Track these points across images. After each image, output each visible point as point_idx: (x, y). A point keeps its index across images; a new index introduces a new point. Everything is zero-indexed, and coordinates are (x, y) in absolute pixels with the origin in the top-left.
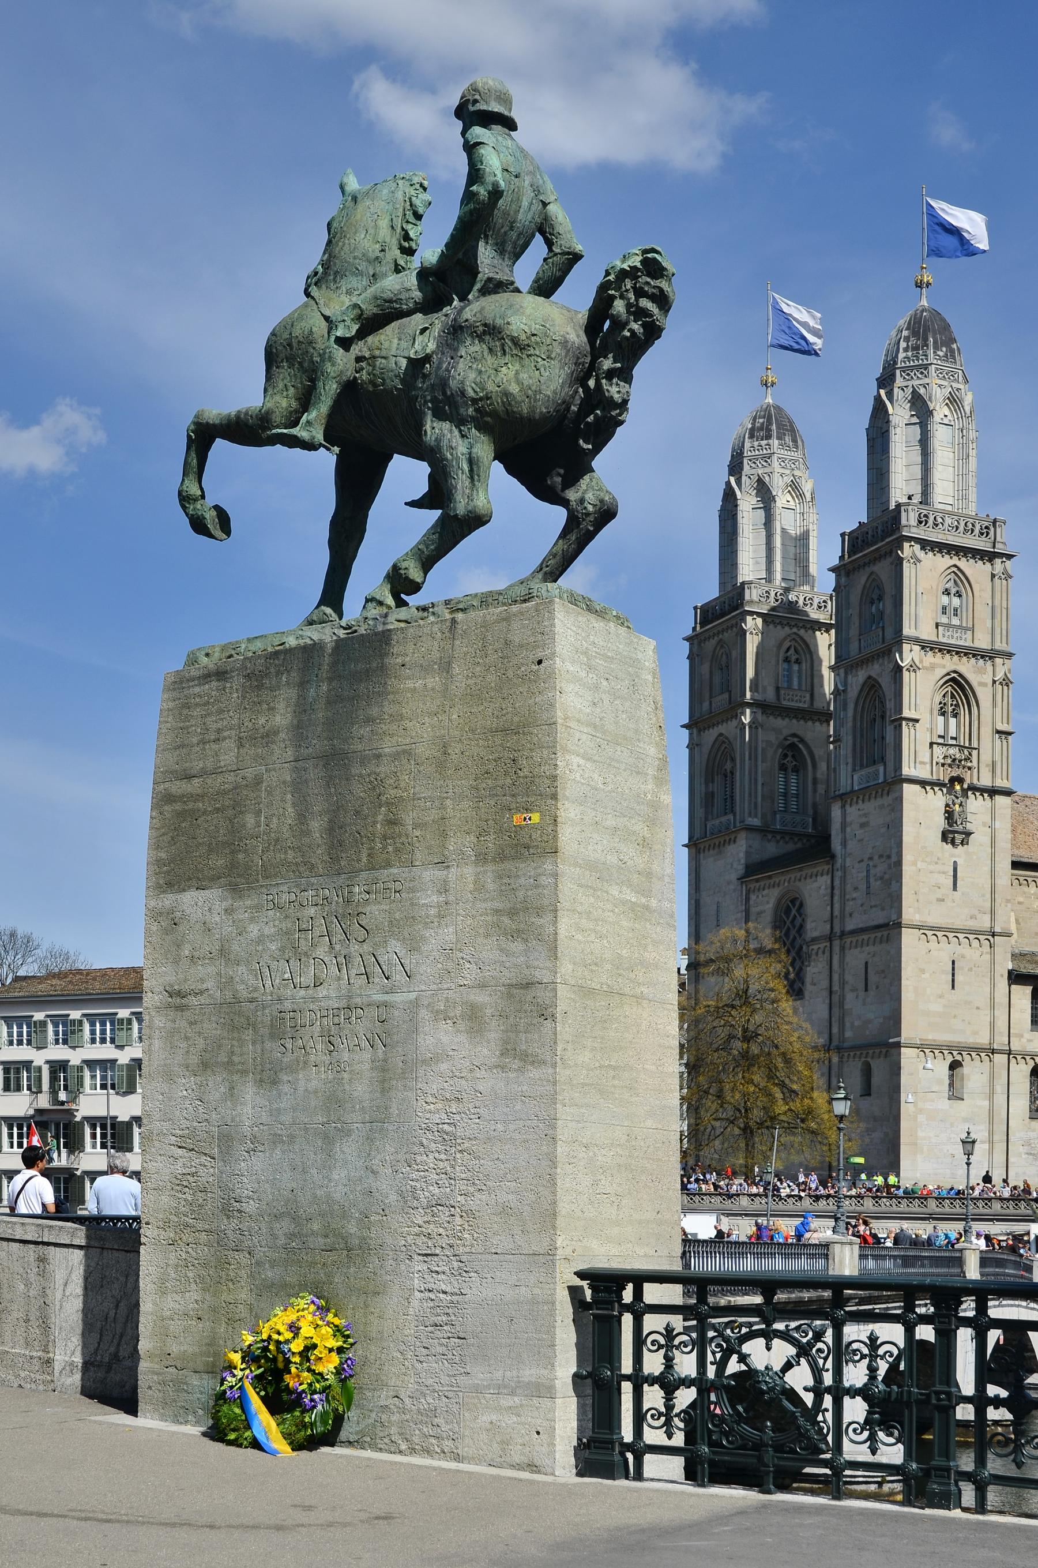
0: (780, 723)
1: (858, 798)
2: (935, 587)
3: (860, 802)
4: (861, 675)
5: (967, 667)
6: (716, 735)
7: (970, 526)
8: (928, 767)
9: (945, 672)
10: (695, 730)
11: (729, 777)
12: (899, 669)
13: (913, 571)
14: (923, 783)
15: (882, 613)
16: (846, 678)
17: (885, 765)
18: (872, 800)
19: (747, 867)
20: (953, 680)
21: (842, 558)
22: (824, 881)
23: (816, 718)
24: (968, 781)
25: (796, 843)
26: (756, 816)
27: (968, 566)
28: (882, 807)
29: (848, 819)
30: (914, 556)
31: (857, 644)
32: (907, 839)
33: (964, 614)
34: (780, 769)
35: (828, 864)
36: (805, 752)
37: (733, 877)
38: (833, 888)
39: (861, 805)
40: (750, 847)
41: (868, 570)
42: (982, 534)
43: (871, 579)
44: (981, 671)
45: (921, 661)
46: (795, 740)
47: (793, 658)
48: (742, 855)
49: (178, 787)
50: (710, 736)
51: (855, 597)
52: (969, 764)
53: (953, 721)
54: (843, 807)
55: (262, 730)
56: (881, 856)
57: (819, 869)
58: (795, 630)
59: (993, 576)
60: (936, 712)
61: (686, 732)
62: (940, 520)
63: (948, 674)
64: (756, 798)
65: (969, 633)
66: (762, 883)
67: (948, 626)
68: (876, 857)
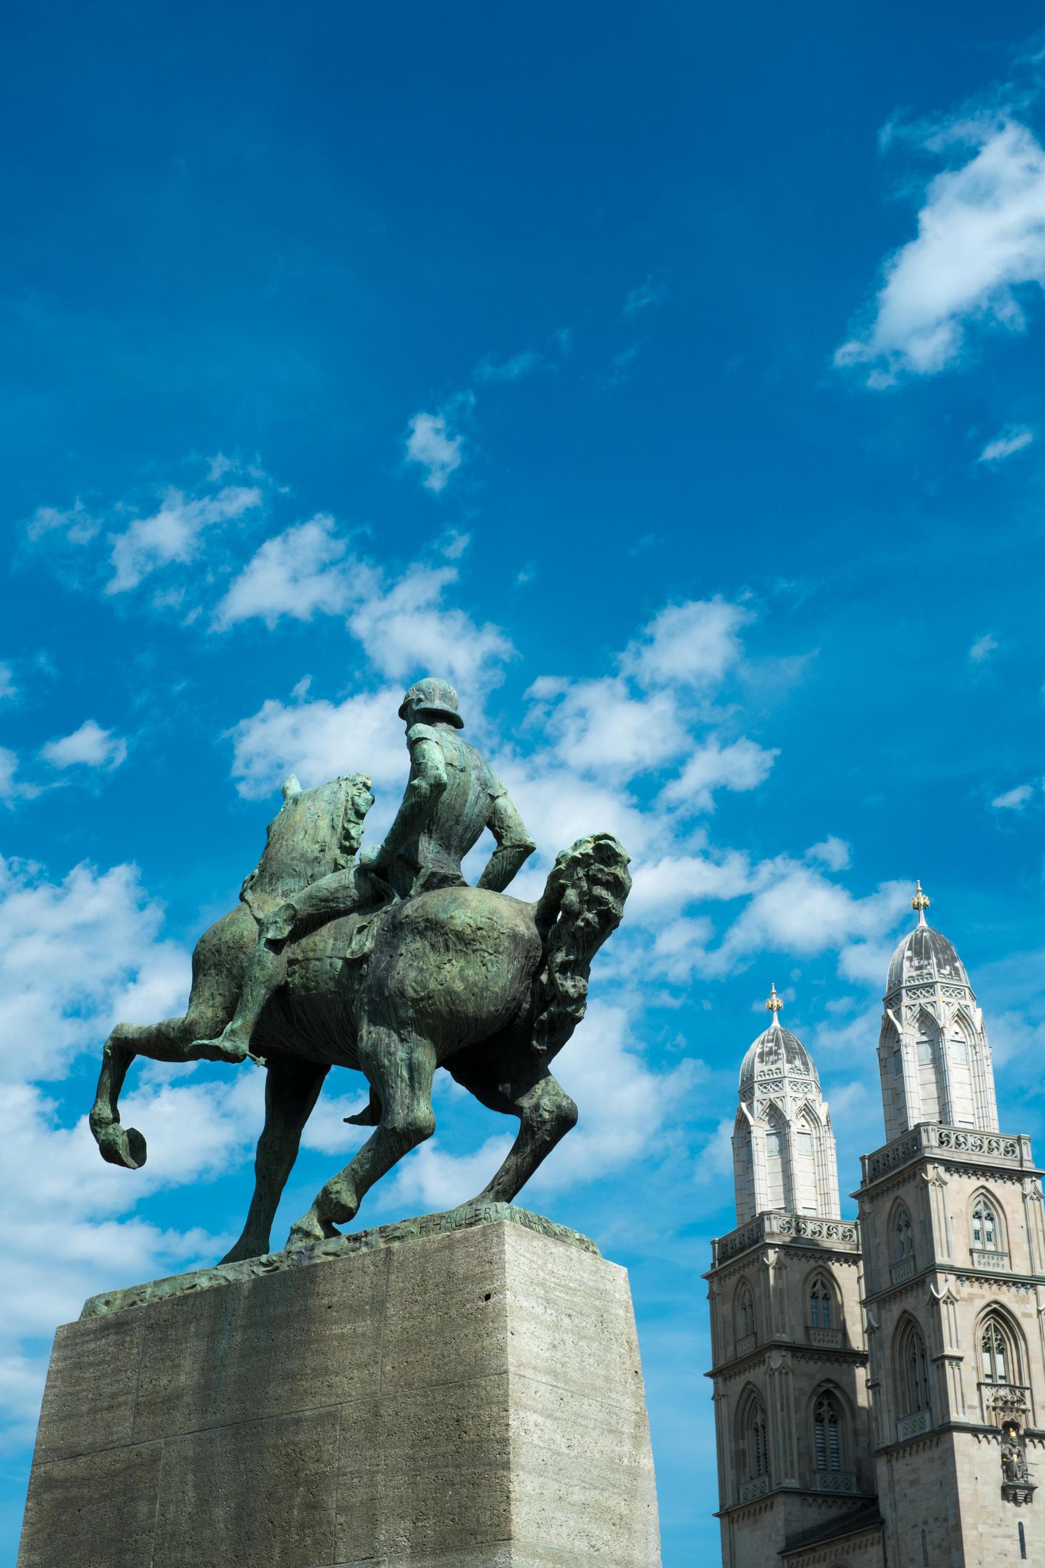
1: (905, 1450)
2: (964, 1210)
3: (907, 1455)
4: (895, 1311)
5: (1008, 1297)
6: (741, 1386)
7: (994, 1145)
8: (978, 1411)
9: (984, 1302)
10: (720, 1379)
11: (760, 1430)
12: (935, 1302)
14: (974, 1431)
15: (911, 1240)
16: (879, 1313)
17: (931, 1411)
18: (921, 1453)
19: (788, 1538)
20: (994, 1311)
21: (863, 1182)
24: (1024, 1426)
25: (840, 1508)
26: (793, 1477)
27: (998, 1187)
29: (896, 1477)
30: (939, 1178)
32: (962, 1497)
33: (999, 1238)
34: (817, 1420)
37: (772, 1551)
38: (886, 1561)
39: (908, 1459)
40: (789, 1513)
41: (892, 1196)
42: (1008, 1152)
43: (896, 1206)
44: (1024, 1301)
45: (958, 1292)
46: (830, 1386)
47: (821, 1294)
48: (780, 1524)
49: (60, 1469)
50: (737, 1384)
51: (881, 1221)
52: (1023, 1407)
53: (999, 1358)
54: (889, 1461)
55: (163, 1393)
56: (936, 1519)
57: (870, 1537)
58: (821, 1263)
59: (1024, 1196)
60: (980, 1349)
61: (710, 1381)
62: (962, 1140)
63: (988, 1305)
64: (792, 1454)
65: (1006, 1259)
66: (806, 1558)
67: (983, 1252)
68: (931, 1521)
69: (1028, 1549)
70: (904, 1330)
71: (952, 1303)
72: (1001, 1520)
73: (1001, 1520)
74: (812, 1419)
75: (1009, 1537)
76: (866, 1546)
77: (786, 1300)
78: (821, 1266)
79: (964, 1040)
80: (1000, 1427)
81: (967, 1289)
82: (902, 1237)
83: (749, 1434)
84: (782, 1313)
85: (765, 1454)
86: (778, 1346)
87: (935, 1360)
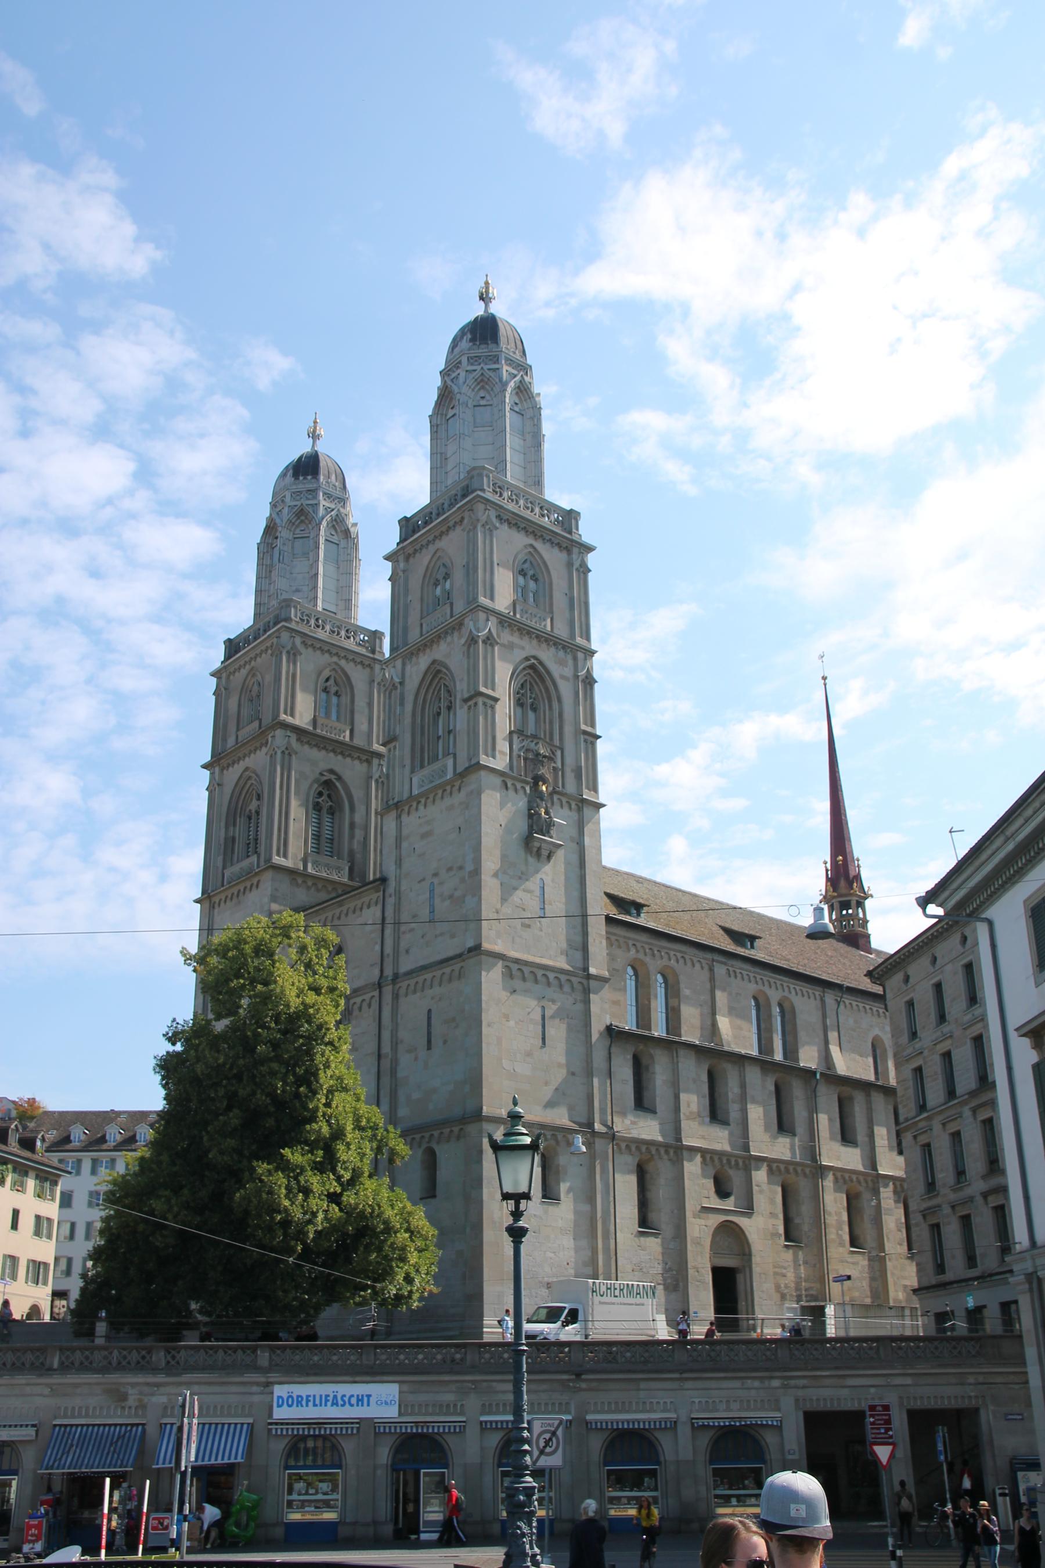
1: (419, 802)
3: (421, 807)
4: (423, 662)
5: (547, 656)
9: (524, 654)
10: (217, 769)
12: (473, 640)
13: (488, 537)
15: (448, 595)
20: (532, 667)
22: (372, 914)
23: (356, 755)
28: (450, 808)
29: (405, 832)
31: (418, 630)
35: (378, 891)
36: (342, 792)
41: (432, 548)
43: (435, 559)
44: (562, 663)
46: (333, 777)
47: (333, 689)
50: (233, 774)
53: (531, 715)
57: (366, 899)
58: (335, 659)
61: (207, 773)
63: (527, 659)
70: (430, 684)
73: (522, 873)
76: (361, 909)
78: (336, 663)
81: (507, 637)
82: (439, 589)
83: (241, 821)
85: (256, 840)
86: (285, 726)
87: (466, 701)
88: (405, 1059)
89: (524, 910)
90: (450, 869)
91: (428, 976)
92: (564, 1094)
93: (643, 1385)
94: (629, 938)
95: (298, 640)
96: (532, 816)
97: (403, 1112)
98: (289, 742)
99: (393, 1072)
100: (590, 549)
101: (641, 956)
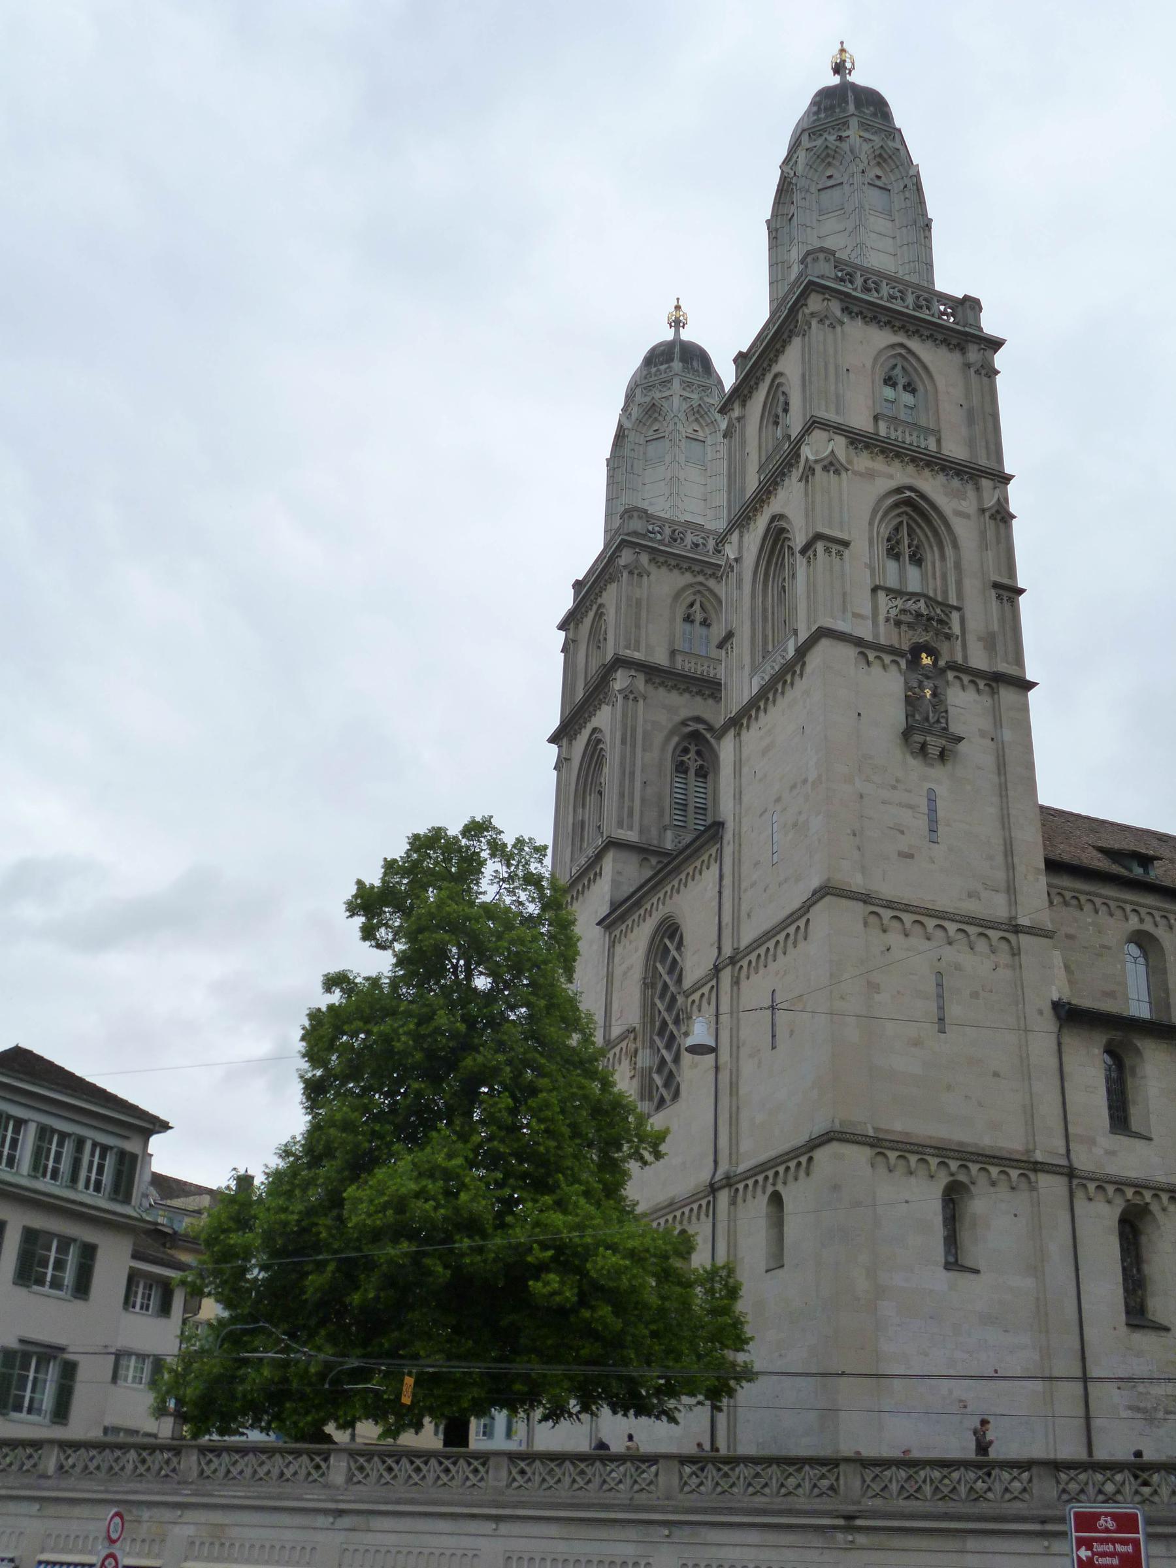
0: (675, 699)
4: (761, 523)
5: (932, 486)
8: (870, 622)
14: (858, 642)
19: (612, 903)
20: (908, 502)
26: (631, 828)
41: (768, 378)
44: (960, 495)
45: (850, 462)
46: (700, 727)
47: (699, 617)
58: (700, 578)
61: (554, 748)
63: (899, 490)
66: (629, 922)
67: (894, 420)
69: (942, 829)
71: (837, 472)
72: (897, 781)
73: (897, 781)
74: (668, 765)
75: (910, 807)
77: (644, 614)
78: (701, 584)
79: (889, 187)
80: (906, 647)
81: (863, 461)
84: (638, 627)
88: (748, 1067)
89: (902, 833)
90: (793, 787)
91: (771, 944)
92: (980, 1105)
93: (972, 1543)
94: (1126, 902)
95: (644, 558)
96: (911, 702)
97: (746, 1145)
98: (631, 684)
99: (734, 1087)
100: (996, 344)
101: (1148, 926)
